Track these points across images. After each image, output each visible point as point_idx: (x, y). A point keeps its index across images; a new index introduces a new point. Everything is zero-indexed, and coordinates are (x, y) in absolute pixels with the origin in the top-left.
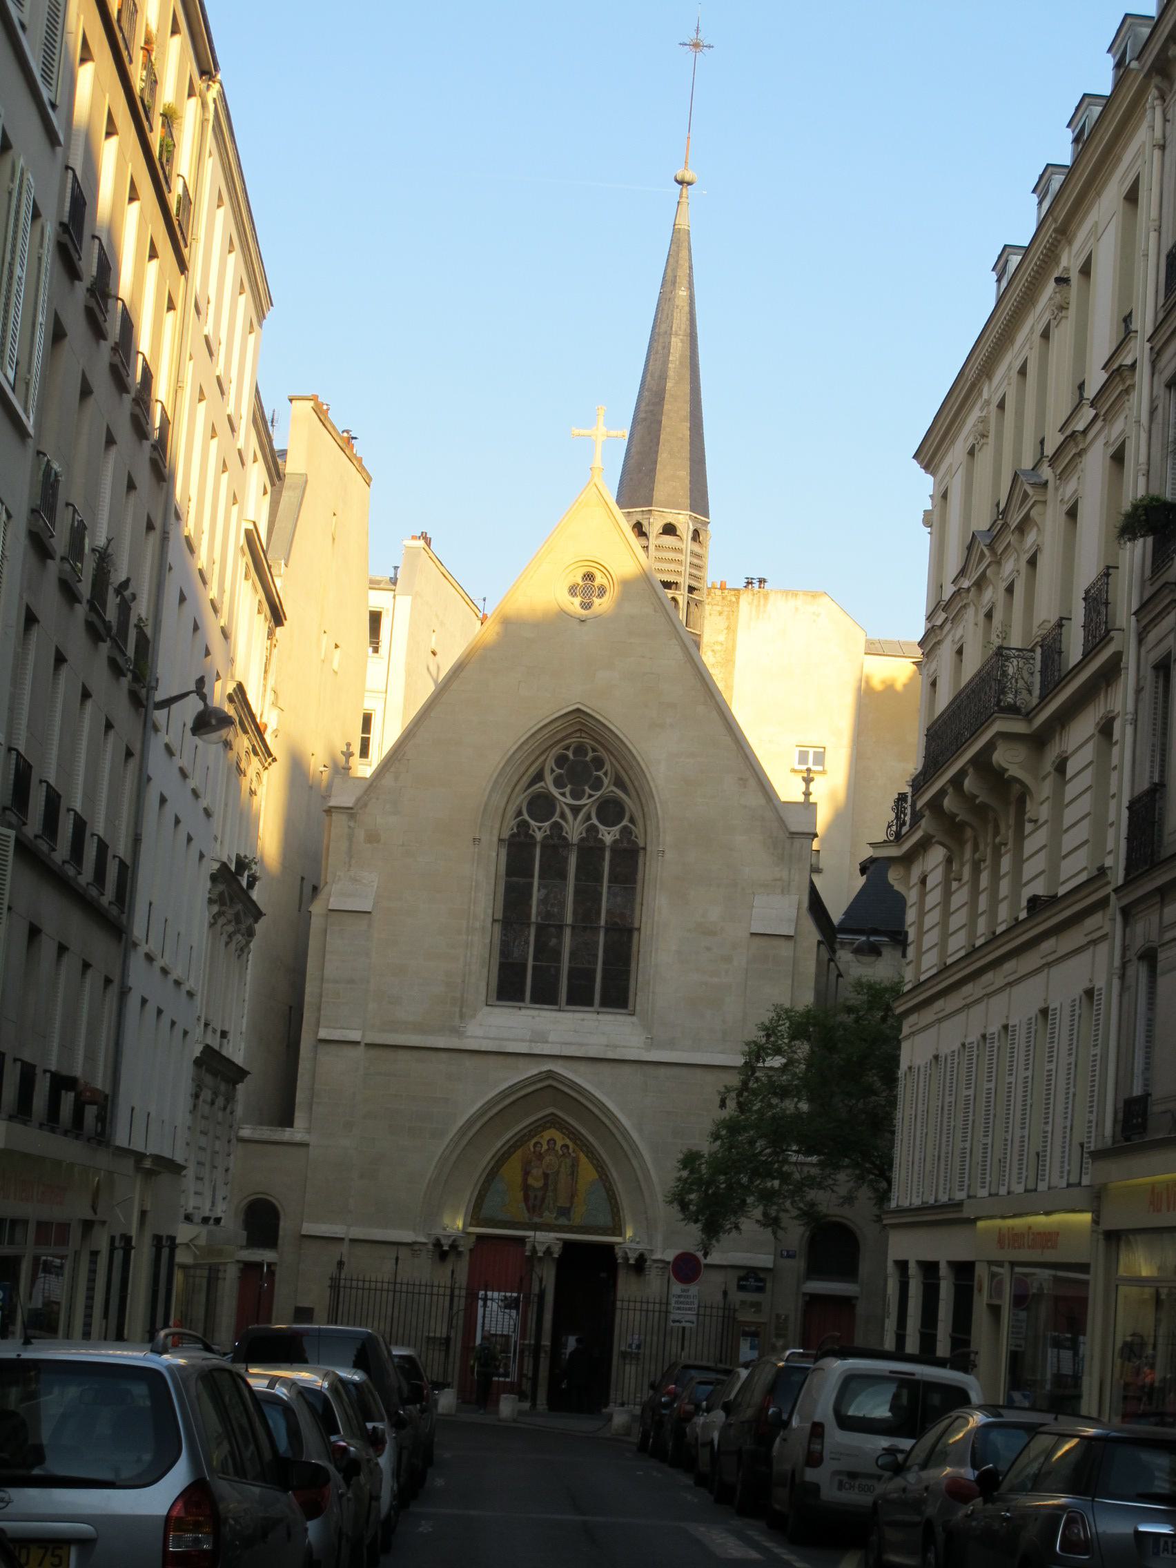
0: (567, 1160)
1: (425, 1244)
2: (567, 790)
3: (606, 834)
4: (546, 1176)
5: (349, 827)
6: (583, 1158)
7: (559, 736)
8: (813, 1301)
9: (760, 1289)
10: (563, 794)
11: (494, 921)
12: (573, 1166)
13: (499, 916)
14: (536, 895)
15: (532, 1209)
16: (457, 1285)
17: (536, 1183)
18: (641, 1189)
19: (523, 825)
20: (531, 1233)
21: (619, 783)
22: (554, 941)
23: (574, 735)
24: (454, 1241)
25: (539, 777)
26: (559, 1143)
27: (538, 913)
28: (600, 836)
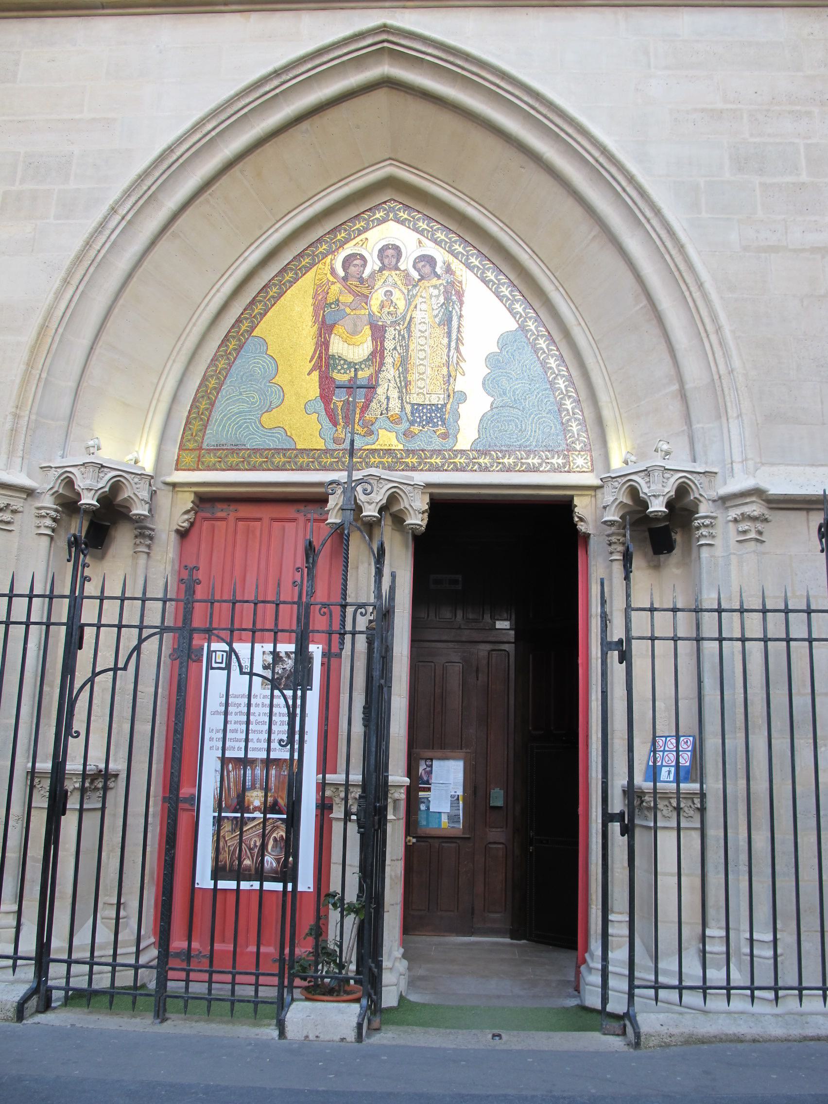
4: (378, 332)
16: (91, 589)
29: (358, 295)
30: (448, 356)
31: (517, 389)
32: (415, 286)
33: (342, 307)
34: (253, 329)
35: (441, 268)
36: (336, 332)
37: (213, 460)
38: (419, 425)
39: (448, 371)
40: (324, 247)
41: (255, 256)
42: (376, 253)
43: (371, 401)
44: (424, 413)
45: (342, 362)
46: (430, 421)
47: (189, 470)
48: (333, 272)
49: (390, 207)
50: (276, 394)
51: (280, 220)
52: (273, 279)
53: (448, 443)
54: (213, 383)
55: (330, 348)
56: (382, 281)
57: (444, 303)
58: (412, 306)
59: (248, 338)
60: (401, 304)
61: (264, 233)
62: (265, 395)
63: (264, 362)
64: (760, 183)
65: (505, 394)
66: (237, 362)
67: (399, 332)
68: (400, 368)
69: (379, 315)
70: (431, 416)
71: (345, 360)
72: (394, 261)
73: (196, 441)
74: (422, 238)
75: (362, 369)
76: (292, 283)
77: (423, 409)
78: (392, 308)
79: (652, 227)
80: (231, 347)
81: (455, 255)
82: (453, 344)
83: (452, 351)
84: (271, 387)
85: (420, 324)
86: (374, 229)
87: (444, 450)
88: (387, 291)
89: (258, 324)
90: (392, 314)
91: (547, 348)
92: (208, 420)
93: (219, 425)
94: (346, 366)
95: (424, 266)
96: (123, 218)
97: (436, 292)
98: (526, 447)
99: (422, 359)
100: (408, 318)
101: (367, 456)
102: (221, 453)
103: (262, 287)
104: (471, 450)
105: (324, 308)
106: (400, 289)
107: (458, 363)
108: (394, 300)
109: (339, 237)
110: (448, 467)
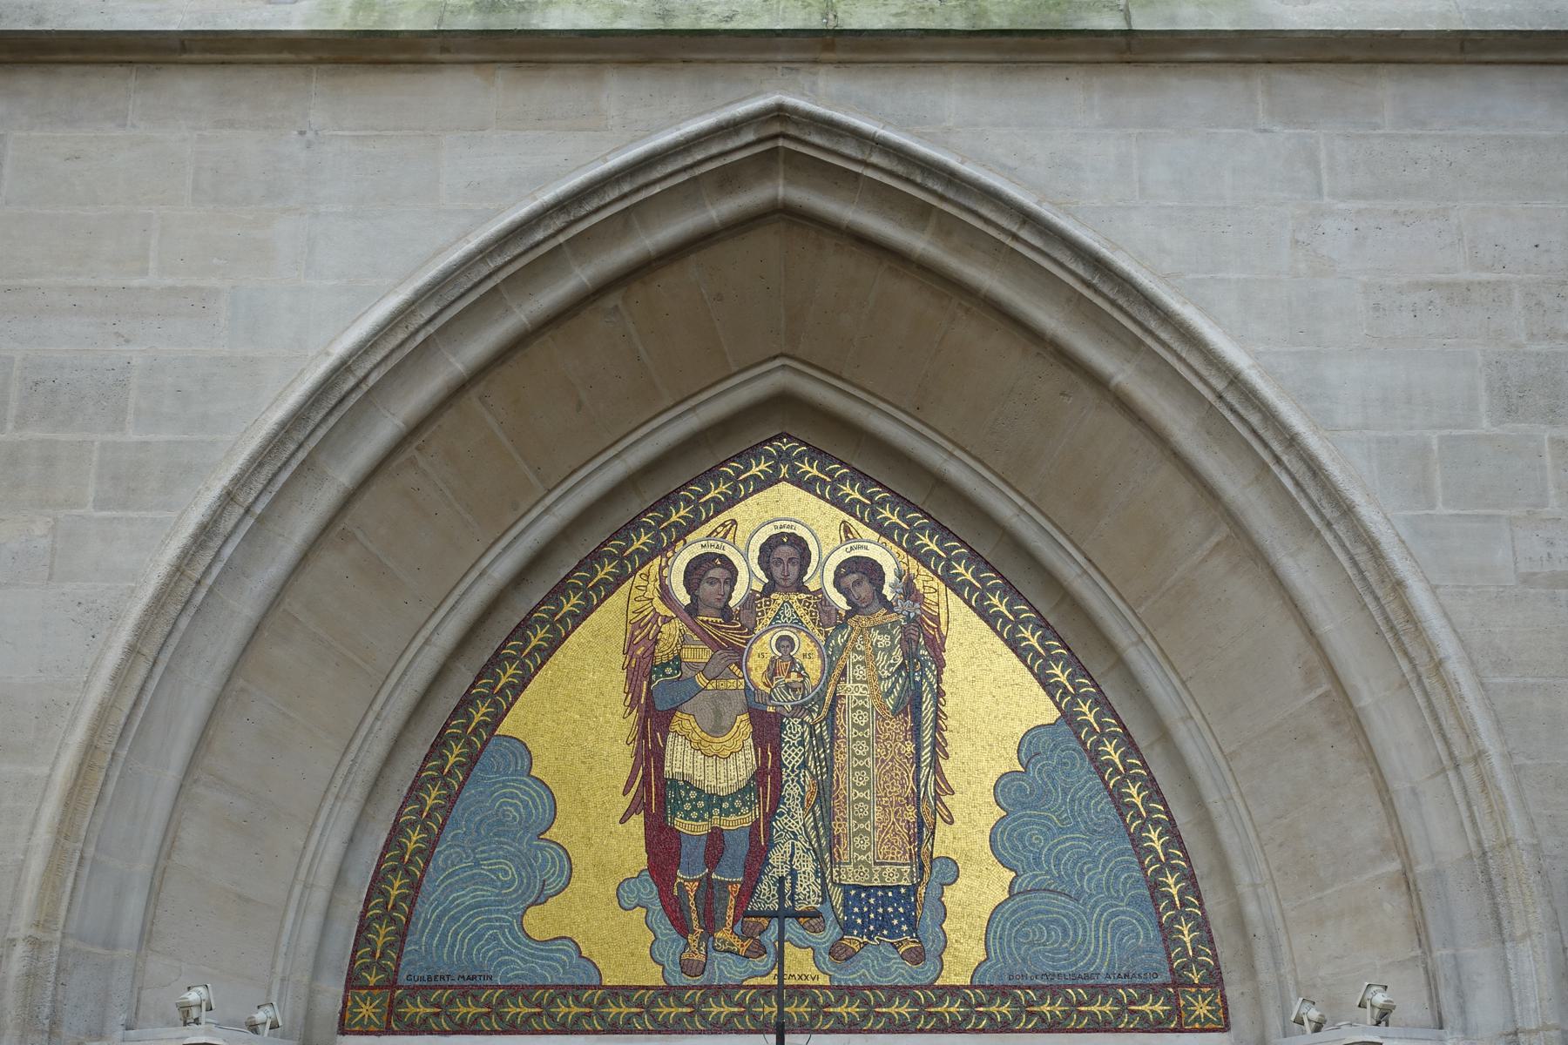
4: (767, 730)
29: (721, 647)
30: (917, 781)
31: (1063, 852)
32: (841, 626)
33: (688, 673)
34: (498, 718)
35: (893, 586)
36: (678, 728)
37: (423, 1010)
38: (861, 934)
39: (918, 813)
40: (642, 541)
41: (503, 567)
42: (754, 554)
43: (759, 881)
44: (869, 905)
45: (693, 794)
46: (884, 922)
47: (367, 1033)
48: (666, 594)
49: (779, 450)
50: (554, 863)
51: (555, 488)
52: (535, 610)
53: (924, 973)
54: (414, 839)
55: (667, 764)
56: (771, 614)
57: (902, 665)
58: (837, 672)
59: (488, 741)
60: (813, 667)
61: (523, 516)
62: (531, 866)
63: (525, 793)
64: (1552, 440)
65: (1038, 863)
66: (465, 794)
67: (812, 728)
68: (817, 808)
69: (768, 690)
70: (885, 911)
71: (699, 791)
72: (794, 570)
73: (383, 969)
74: (853, 521)
75: (737, 811)
77: (868, 897)
78: (794, 676)
79: (1337, 537)
80: (452, 760)
81: (923, 559)
82: (926, 754)
83: (925, 771)
84: (542, 849)
85: (854, 710)
86: (749, 500)
87: (916, 987)
88: (782, 638)
89: (508, 710)
90: (794, 690)
91: (1123, 762)
92: (408, 921)
93: (432, 935)
94: (701, 804)
95: (857, 583)
96: (247, 511)
97: (884, 641)
98: (1087, 977)
99: (862, 789)
100: (828, 698)
101: (754, 1001)
102: (441, 996)
103: (513, 626)
104: (972, 987)
105: (650, 674)
106: (809, 635)
107: (937, 797)
108: (799, 658)
109: (674, 518)
110: (926, 1023)
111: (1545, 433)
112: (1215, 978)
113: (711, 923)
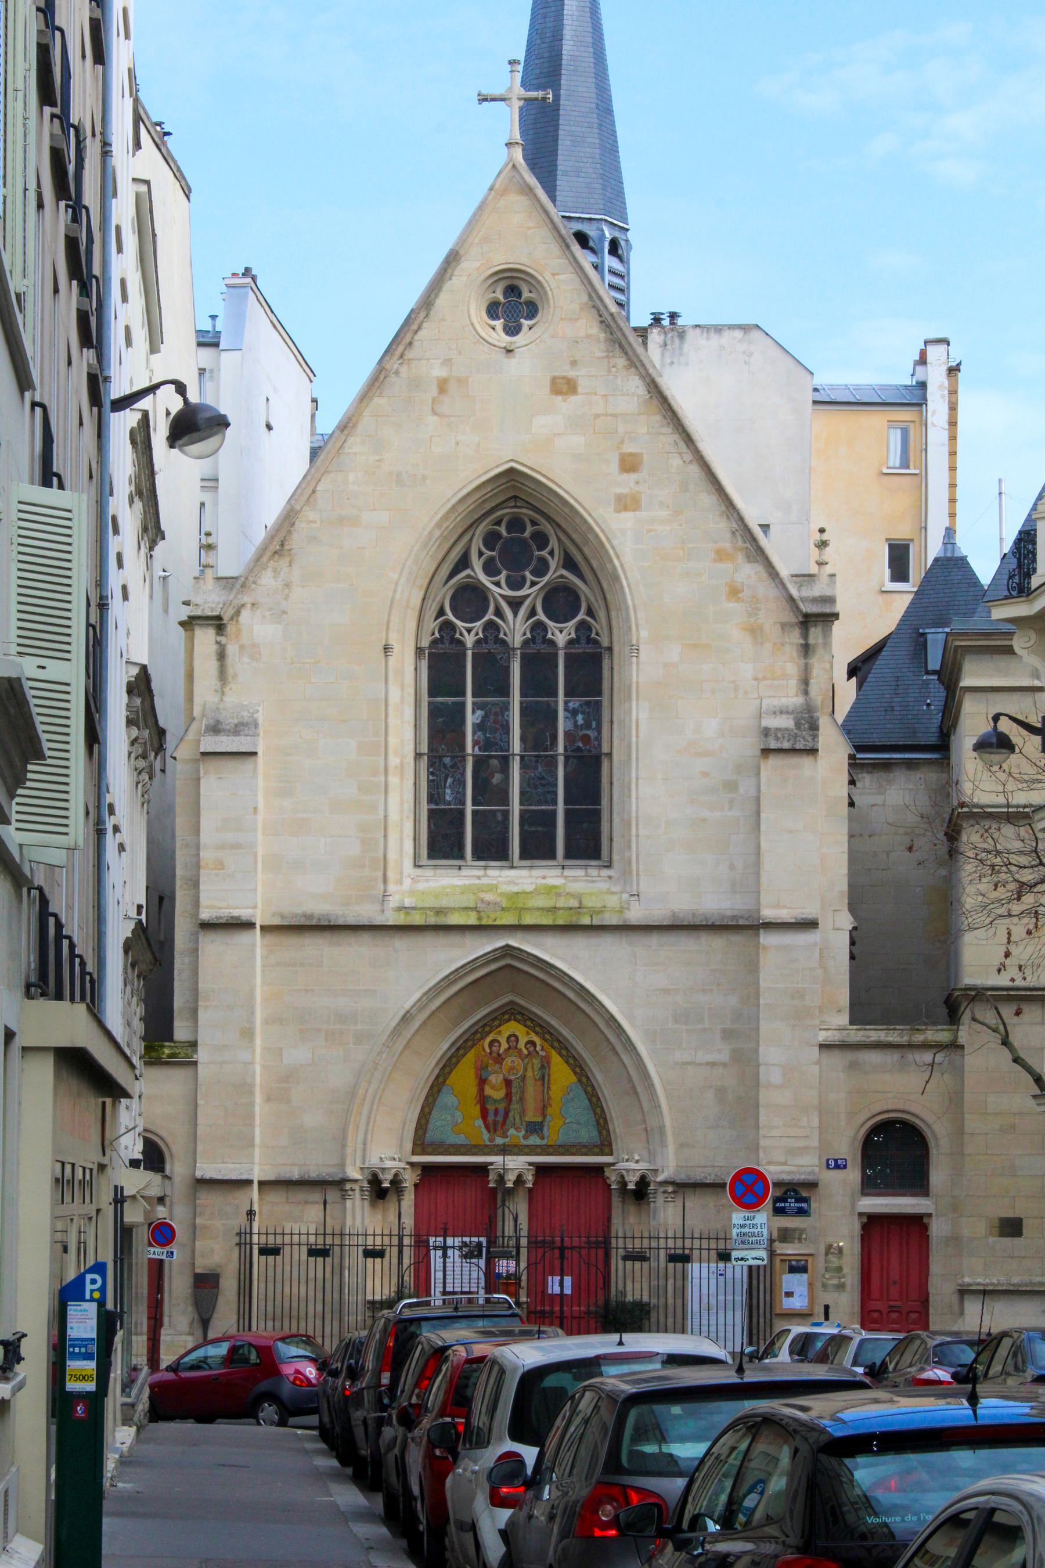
0: (535, 1061)
1: (356, 1181)
2: (502, 577)
3: (557, 632)
4: (508, 1083)
5: (217, 643)
6: (556, 1059)
7: (488, 506)
8: (872, 1223)
9: (802, 1212)
10: (498, 584)
11: (418, 756)
12: (543, 1067)
13: (424, 748)
14: (471, 718)
15: (492, 1128)
17: (495, 1092)
18: (636, 1093)
19: (447, 627)
20: (497, 1159)
21: (569, 563)
22: (497, 778)
23: (505, 505)
24: (396, 1175)
25: (464, 562)
26: (523, 1041)
27: (475, 743)
28: (549, 636)
48: (484, 1050)
53: (544, 1142)
76: (464, 1055)
81: (546, 1040)
111: (684, 1027)
112: (610, 1145)
113: (495, 1131)
